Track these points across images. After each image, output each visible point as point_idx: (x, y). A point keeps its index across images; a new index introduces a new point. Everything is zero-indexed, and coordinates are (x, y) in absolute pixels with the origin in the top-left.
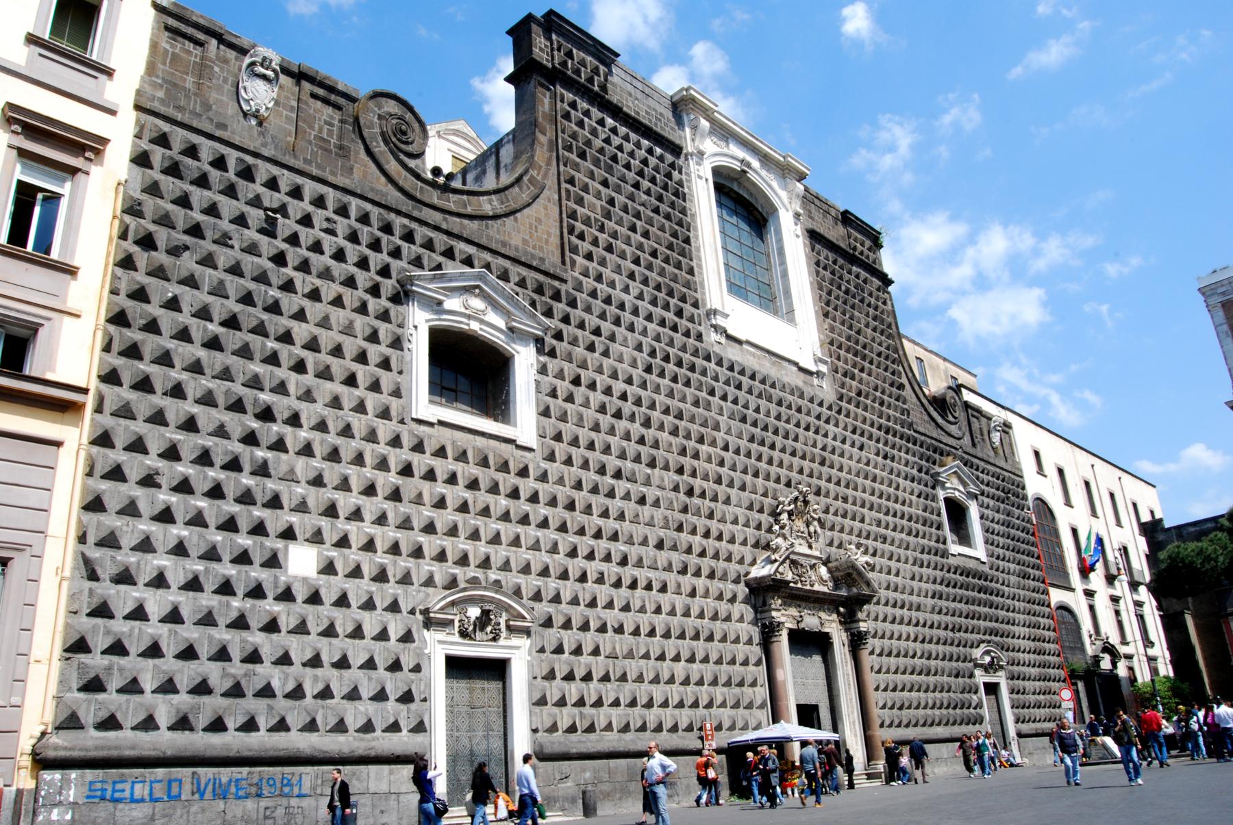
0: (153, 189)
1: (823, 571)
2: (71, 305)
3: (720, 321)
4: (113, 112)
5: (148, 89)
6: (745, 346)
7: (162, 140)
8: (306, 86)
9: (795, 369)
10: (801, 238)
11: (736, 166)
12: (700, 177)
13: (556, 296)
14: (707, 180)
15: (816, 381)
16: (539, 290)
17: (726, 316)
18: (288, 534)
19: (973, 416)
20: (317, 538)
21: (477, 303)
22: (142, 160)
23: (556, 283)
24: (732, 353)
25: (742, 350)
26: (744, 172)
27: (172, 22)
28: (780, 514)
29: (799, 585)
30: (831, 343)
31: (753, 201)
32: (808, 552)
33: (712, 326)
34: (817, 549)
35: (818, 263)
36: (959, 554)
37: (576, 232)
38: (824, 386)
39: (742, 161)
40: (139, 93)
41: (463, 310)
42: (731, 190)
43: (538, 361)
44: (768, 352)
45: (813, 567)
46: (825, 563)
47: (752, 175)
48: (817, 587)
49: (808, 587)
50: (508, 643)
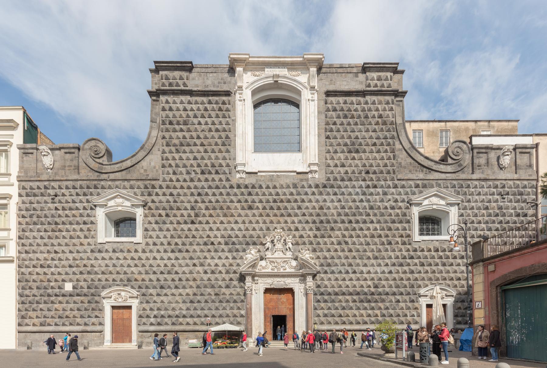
0: (23, 203)
1: (294, 263)
2: (11, 238)
3: (239, 168)
4: (13, 185)
5: (20, 175)
6: (259, 174)
7: (24, 188)
8: (63, 151)
9: (295, 174)
10: (316, 102)
11: (270, 81)
12: (240, 101)
13: (153, 187)
14: (244, 100)
15: (310, 176)
16: (146, 187)
17: (244, 165)
18: (63, 281)
19: (478, 153)
20: (71, 280)
21: (119, 200)
22: (20, 195)
23: (153, 182)
24: (251, 180)
26: (276, 81)
27: (22, 151)
29: (276, 271)
30: (329, 152)
32: (285, 256)
33: (237, 172)
36: (422, 240)
37: (164, 158)
38: (317, 176)
39: (273, 77)
40: (18, 177)
41: (115, 205)
43: (144, 212)
46: (296, 259)
47: (281, 81)
48: (288, 270)
49: (282, 270)
50: (131, 301)
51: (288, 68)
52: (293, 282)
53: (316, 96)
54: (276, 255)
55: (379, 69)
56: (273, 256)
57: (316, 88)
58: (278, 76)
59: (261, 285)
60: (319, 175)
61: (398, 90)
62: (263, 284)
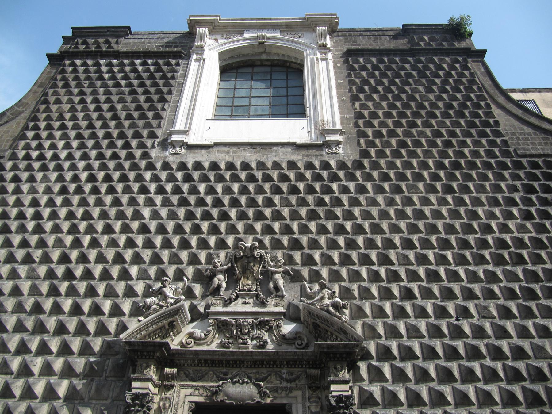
14: (204, 60)
25: (209, 153)
26: (263, 43)
28: (214, 275)
31: (286, 59)
34: (276, 305)
35: (352, 68)
38: (341, 151)
42: (261, 60)
44: (252, 145)
45: (261, 325)
51: (281, 31)
52: (284, 384)
53: (330, 56)
54: (238, 306)
55: (430, 31)
56: (230, 309)
57: (329, 46)
58: (265, 37)
59: (184, 392)
60: (345, 150)
61: (471, 48)
62: (189, 391)
